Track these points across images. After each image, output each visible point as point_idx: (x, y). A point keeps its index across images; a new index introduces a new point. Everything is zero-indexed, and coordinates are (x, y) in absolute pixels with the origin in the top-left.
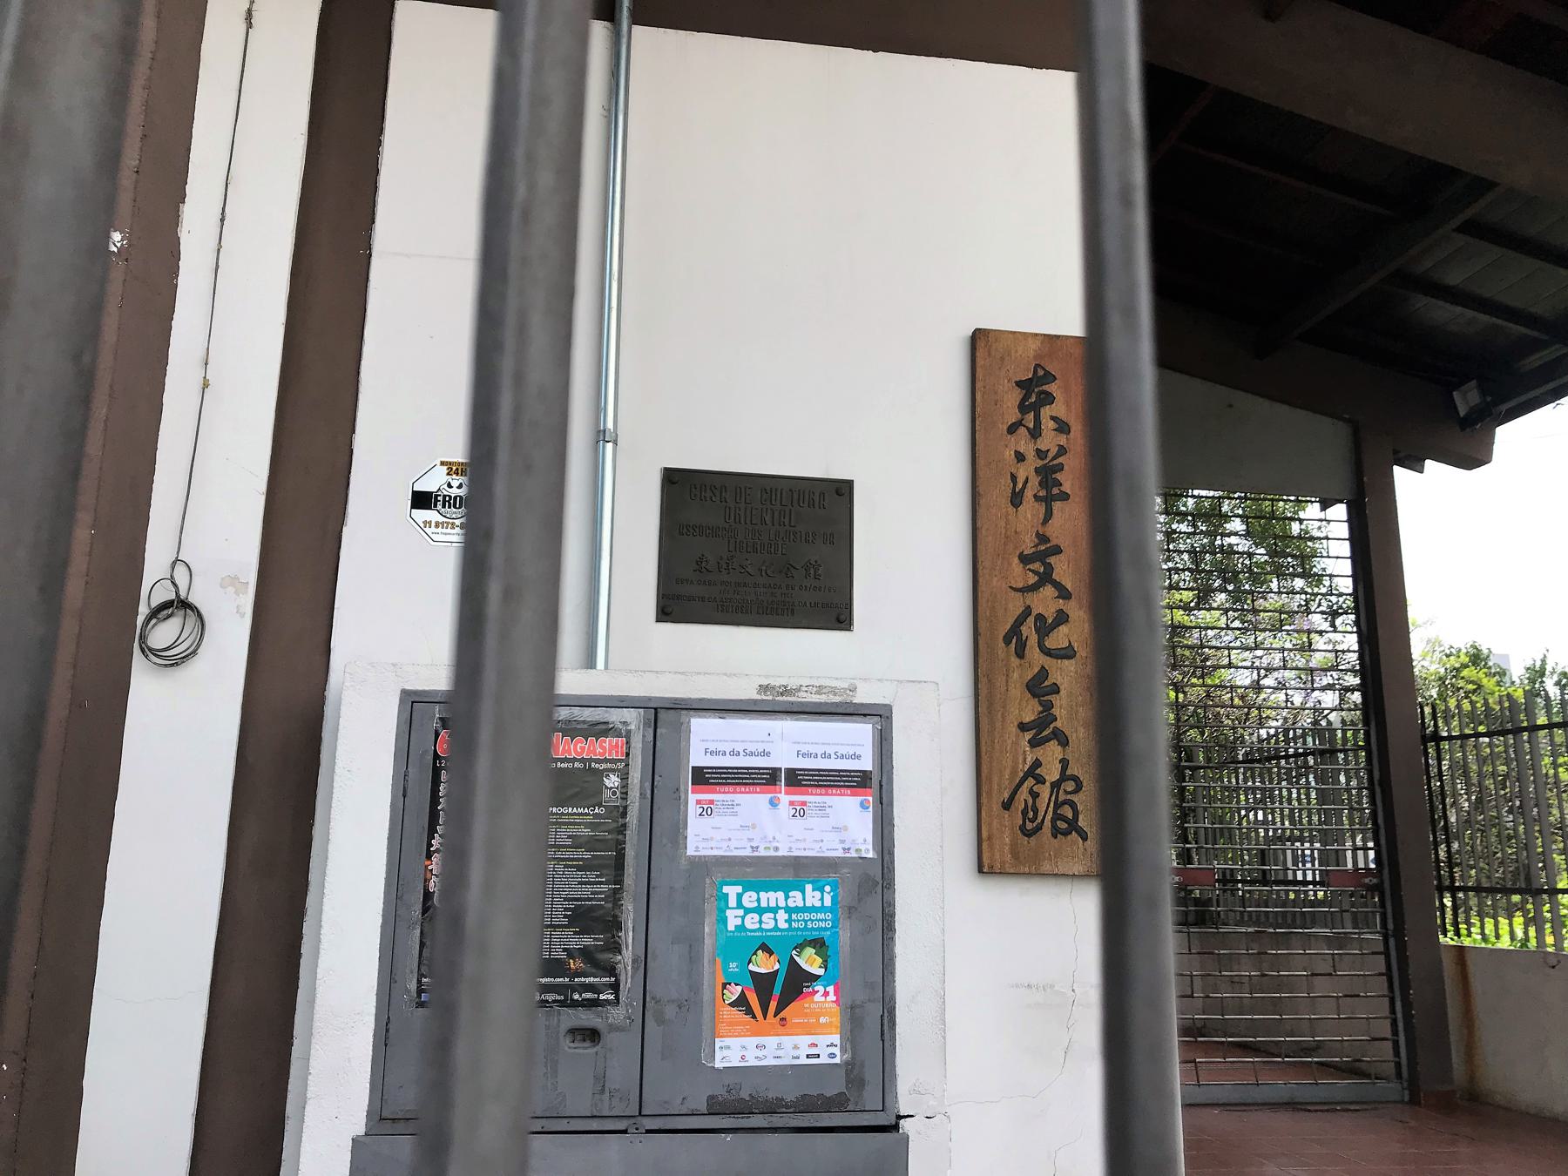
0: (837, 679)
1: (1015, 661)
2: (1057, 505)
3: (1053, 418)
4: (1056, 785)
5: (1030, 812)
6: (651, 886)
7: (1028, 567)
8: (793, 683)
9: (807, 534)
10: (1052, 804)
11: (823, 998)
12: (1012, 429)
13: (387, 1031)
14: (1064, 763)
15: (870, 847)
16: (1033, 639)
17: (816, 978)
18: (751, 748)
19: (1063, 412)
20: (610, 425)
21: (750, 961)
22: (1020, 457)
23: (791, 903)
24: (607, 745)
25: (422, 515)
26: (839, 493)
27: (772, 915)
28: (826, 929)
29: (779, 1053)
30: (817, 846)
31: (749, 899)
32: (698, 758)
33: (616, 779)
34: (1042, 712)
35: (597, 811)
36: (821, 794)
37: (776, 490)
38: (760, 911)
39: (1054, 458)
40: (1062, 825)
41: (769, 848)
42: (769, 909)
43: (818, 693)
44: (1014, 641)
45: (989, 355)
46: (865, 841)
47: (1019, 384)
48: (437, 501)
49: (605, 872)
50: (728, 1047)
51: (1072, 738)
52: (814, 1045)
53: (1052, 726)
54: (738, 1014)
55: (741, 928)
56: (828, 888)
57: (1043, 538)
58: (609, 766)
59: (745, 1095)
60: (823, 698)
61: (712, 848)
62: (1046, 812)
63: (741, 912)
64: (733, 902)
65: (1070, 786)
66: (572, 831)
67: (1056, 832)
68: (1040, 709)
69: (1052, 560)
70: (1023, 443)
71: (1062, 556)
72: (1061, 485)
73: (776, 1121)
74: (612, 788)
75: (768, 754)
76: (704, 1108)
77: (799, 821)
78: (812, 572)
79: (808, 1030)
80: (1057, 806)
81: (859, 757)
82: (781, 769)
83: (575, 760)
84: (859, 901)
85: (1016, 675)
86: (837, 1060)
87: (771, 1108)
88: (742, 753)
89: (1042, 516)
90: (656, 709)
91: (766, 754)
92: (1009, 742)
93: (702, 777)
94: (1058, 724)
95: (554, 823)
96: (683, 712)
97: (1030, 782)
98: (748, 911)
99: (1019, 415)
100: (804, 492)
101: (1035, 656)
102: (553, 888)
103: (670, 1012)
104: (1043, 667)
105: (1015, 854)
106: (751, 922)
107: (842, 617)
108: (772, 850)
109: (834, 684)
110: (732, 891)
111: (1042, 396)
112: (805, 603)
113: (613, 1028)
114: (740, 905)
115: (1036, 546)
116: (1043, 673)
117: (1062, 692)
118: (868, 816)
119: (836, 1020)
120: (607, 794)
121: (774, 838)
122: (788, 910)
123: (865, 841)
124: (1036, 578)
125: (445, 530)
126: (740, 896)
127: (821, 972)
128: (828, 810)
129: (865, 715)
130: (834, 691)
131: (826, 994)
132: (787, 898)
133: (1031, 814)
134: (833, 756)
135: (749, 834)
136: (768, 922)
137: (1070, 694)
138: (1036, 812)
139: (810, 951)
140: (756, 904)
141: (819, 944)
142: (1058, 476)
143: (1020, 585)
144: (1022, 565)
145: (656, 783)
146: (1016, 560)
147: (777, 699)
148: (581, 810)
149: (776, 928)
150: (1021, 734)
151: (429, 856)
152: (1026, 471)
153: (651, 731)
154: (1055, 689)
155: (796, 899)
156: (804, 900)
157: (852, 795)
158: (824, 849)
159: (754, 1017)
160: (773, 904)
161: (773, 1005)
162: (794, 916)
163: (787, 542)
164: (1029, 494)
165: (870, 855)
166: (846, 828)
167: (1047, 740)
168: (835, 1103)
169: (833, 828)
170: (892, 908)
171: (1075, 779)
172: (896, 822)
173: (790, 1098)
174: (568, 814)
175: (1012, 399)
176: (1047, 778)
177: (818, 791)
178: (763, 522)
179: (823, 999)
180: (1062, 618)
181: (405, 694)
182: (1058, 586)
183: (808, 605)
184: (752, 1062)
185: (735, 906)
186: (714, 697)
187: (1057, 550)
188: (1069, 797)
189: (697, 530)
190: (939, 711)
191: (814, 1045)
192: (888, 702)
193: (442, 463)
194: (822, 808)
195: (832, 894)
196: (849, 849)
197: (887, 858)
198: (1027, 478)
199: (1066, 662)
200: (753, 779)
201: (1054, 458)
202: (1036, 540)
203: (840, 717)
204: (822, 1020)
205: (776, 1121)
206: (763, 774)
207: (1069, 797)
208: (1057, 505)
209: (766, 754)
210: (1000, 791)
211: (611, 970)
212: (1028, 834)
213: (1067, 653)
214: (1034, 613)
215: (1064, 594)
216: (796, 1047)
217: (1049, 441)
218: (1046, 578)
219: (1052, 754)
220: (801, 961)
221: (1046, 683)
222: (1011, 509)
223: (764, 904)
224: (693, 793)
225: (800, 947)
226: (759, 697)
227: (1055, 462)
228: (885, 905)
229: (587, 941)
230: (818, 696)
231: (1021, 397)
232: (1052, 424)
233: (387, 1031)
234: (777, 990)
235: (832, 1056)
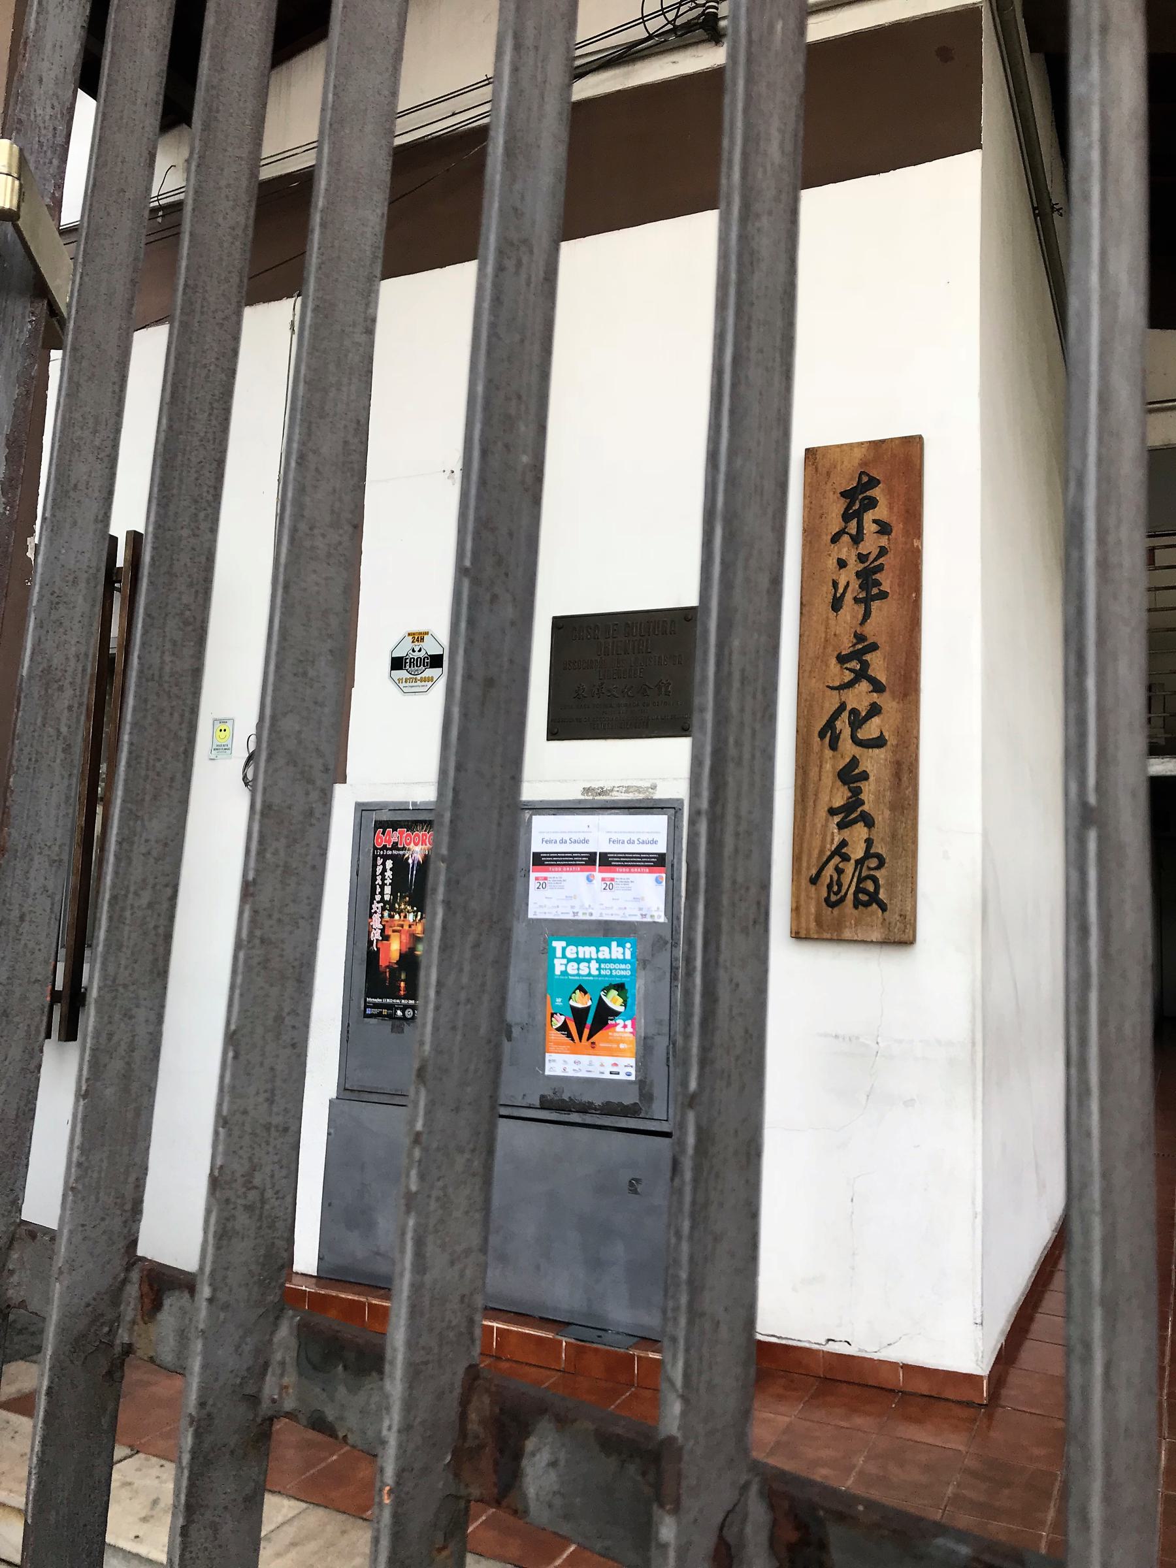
1: (828, 753)
2: (875, 605)
3: (875, 521)
4: (860, 863)
7: (845, 666)
8: (607, 786)
10: (855, 880)
11: (622, 1030)
12: (835, 539)
13: (348, 1032)
14: (869, 842)
15: (663, 914)
16: (847, 732)
17: (616, 1014)
18: (575, 837)
19: (885, 513)
21: (571, 998)
22: (842, 564)
23: (601, 956)
25: (398, 674)
27: (586, 964)
28: (626, 977)
29: (590, 1068)
31: (571, 952)
32: (537, 846)
34: (851, 798)
38: (578, 961)
39: (875, 560)
42: (584, 960)
43: (626, 792)
44: (829, 734)
45: (817, 471)
47: (844, 494)
48: (406, 663)
50: (554, 1061)
51: (878, 819)
52: (615, 1065)
53: (859, 810)
54: (561, 1037)
55: (565, 973)
56: (628, 945)
57: (860, 638)
59: (565, 1097)
60: (630, 796)
62: (849, 886)
63: (565, 961)
65: (873, 863)
67: (857, 903)
68: (850, 794)
69: (868, 657)
70: (845, 550)
71: (878, 653)
72: (880, 584)
73: (588, 1119)
75: (587, 842)
76: (537, 1104)
78: (663, 689)
79: (611, 1052)
80: (860, 881)
81: (656, 842)
82: (595, 853)
85: (828, 767)
86: (633, 1078)
87: (585, 1109)
89: (860, 617)
91: (586, 841)
92: (819, 825)
93: (540, 860)
94: (866, 808)
97: (837, 859)
98: (569, 960)
99: (843, 524)
101: (848, 748)
103: (516, 1032)
104: (854, 757)
105: (819, 922)
106: (572, 969)
109: (639, 784)
110: (558, 945)
111: (866, 502)
114: (564, 956)
115: (854, 645)
116: (854, 762)
117: (872, 778)
122: (598, 961)
124: (852, 675)
125: (411, 684)
126: (564, 949)
127: (621, 1009)
128: (631, 885)
129: (662, 808)
130: (638, 790)
131: (625, 1026)
132: (598, 951)
133: (835, 888)
136: (584, 970)
137: (878, 781)
138: (840, 885)
139: (613, 993)
140: (575, 956)
141: (620, 988)
142: (877, 576)
143: (837, 684)
144: (839, 666)
146: (834, 661)
149: (589, 974)
150: (831, 818)
151: (371, 917)
152: (846, 576)
154: (865, 776)
155: (604, 953)
159: (573, 1040)
160: (587, 956)
161: (586, 1032)
162: (603, 966)
164: (849, 597)
165: (662, 919)
166: (643, 899)
167: (854, 822)
171: (878, 856)
173: (598, 1102)
175: (836, 508)
176: (852, 856)
179: (622, 1030)
180: (875, 710)
181: (358, 805)
184: (570, 1073)
187: (874, 647)
188: (872, 873)
191: (615, 1065)
193: (409, 634)
194: (626, 882)
197: (675, 922)
198: (848, 583)
199: (876, 751)
201: (875, 560)
202: (855, 641)
204: (622, 1046)
205: (588, 1119)
207: (872, 873)
208: (875, 605)
209: (586, 841)
210: (808, 868)
213: (878, 742)
214: (849, 707)
215: (878, 687)
216: (602, 1065)
217: (871, 543)
218: (862, 674)
219: (860, 832)
220: (607, 1000)
221: (857, 771)
222: (832, 614)
223: (581, 956)
225: (607, 989)
226: (582, 797)
227: (876, 563)
231: (845, 506)
232: (874, 527)
233: (348, 1032)
234: (589, 1021)
235: (629, 1074)
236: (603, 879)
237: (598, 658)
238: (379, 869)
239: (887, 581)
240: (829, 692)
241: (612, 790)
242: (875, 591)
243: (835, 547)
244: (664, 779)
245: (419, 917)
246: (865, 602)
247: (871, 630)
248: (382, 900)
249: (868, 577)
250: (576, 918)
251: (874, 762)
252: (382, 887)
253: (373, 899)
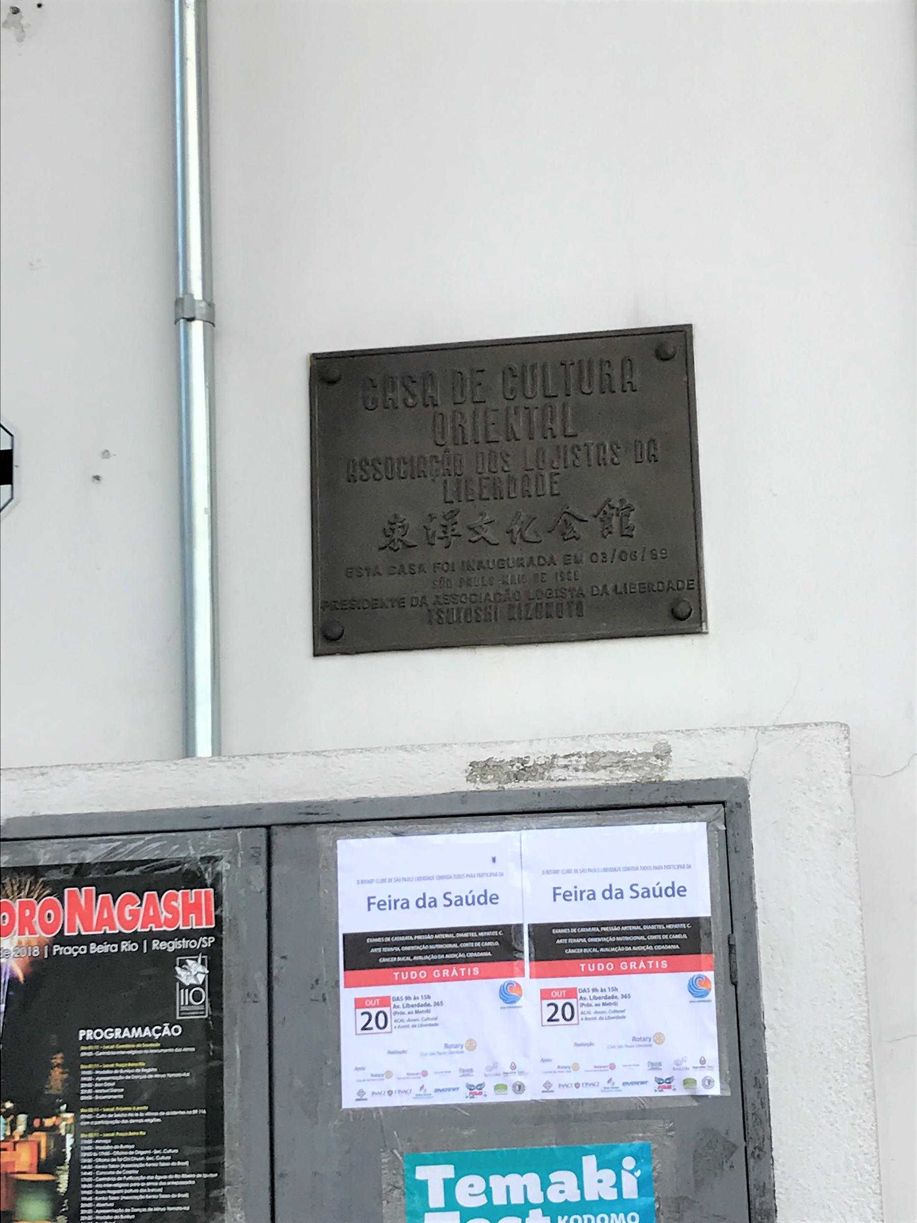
0: (628, 736)
6: (277, 1172)
8: (537, 753)
9: (601, 446)
15: (715, 1075)
18: (459, 888)
20: (197, 290)
23: (554, 1196)
24: (178, 904)
26: (663, 356)
30: (602, 1078)
33: (200, 968)
35: (166, 1031)
36: (606, 973)
37: (533, 367)
41: (505, 1087)
43: (590, 768)
46: (703, 1061)
49: (189, 1151)
56: (629, 1163)
58: (185, 944)
60: (601, 778)
61: (390, 1093)
64: (436, 1198)
66: (125, 1072)
74: (191, 987)
75: (493, 899)
77: (562, 1029)
78: (615, 521)
81: (681, 891)
82: (519, 927)
83: (117, 938)
84: (699, 1184)
88: (441, 901)
90: (268, 827)
95: (87, 1061)
96: (323, 828)
100: (590, 362)
102: (94, 1183)
107: (682, 609)
108: (510, 1088)
109: (624, 746)
112: (605, 587)
114: (451, 1204)
118: (708, 1010)
120: (183, 998)
121: (513, 1067)
123: (703, 1061)
126: (449, 1186)
128: (622, 1004)
129: (690, 805)
130: (622, 761)
132: (545, 1185)
134: (628, 893)
135: (465, 1060)
140: (482, 1201)
145: (275, 972)
147: (506, 787)
148: (137, 1033)
153: (261, 870)
156: (581, 1187)
157: (671, 969)
158: (618, 1084)
160: (517, 1199)
163: (561, 470)
165: (715, 1090)
166: (659, 1039)
169: (634, 1039)
170: (768, 1197)
172: (769, 1018)
174: (114, 1041)
177: (601, 966)
178: (511, 436)
183: (610, 588)
185: (443, 1206)
186: (383, 795)
189: (381, 468)
190: (850, 783)
192: (735, 773)
194: (609, 999)
195: (638, 1174)
196: (669, 1080)
197: (751, 1094)
200: (465, 950)
203: (640, 813)
206: (486, 939)
223: (499, 1199)
224: (346, 986)
226: (471, 787)
228: (753, 1192)
230: (591, 775)
236: (545, 994)
237: (439, 452)
241: (550, 765)
244: (688, 732)
245: (21, 1128)
250: (478, 1100)
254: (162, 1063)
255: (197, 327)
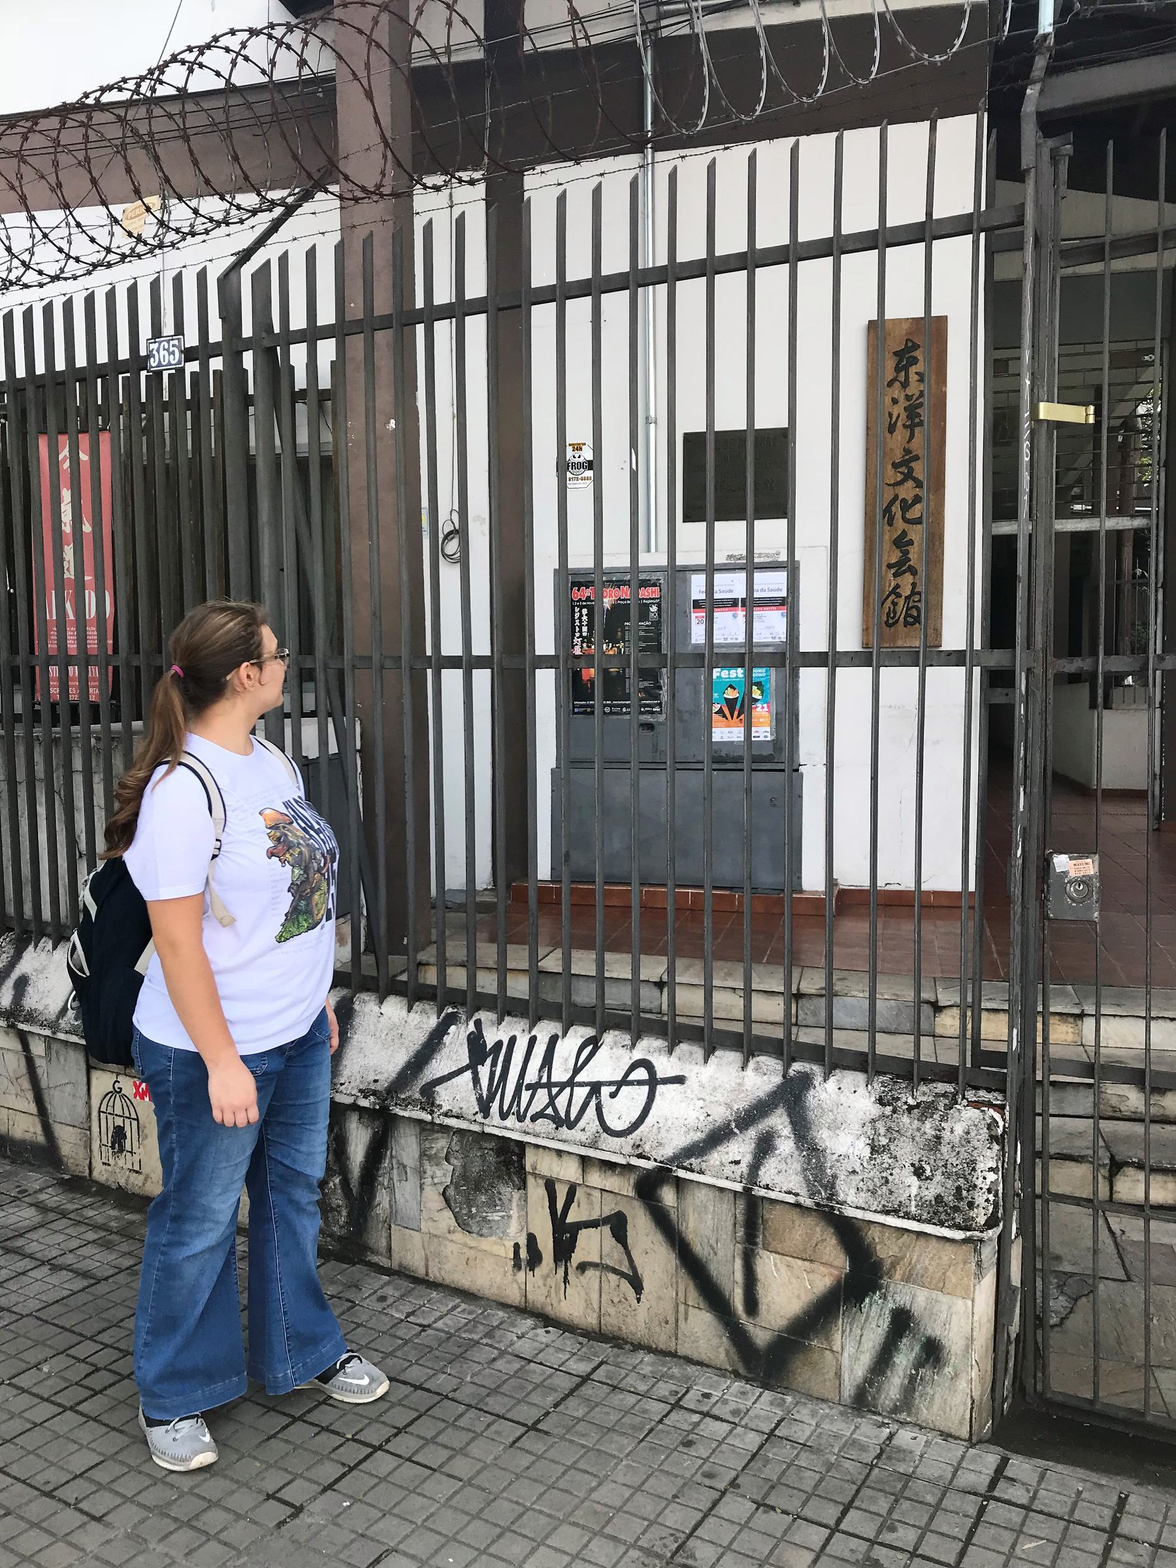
1: (887, 528)
2: (917, 430)
4: (908, 598)
5: (892, 614)
12: (890, 384)
14: (914, 585)
16: (899, 514)
22: (895, 401)
40: (910, 620)
47: (895, 353)
57: (907, 451)
59: (723, 754)
67: (906, 624)
69: (913, 464)
70: (896, 392)
71: (919, 462)
85: (887, 537)
86: (769, 739)
91: (731, 591)
94: (911, 563)
101: (900, 524)
103: (686, 716)
113: (660, 724)
116: (904, 533)
117: (916, 544)
119: (767, 720)
120: (652, 615)
130: (767, 555)
138: (895, 613)
154: (911, 543)
161: (736, 713)
164: (899, 424)
167: (904, 572)
168: (768, 759)
171: (919, 593)
175: (890, 364)
180: (917, 499)
182: (915, 480)
184: (726, 739)
187: (917, 458)
208: (917, 430)
209: (731, 591)
211: (657, 697)
212: (889, 626)
213: (918, 521)
215: (919, 485)
217: (914, 389)
218: (909, 476)
219: (908, 578)
229: (646, 684)
232: (916, 377)
238: (577, 615)
239: (924, 412)
240: (887, 488)
242: (917, 420)
243: (890, 390)
246: (911, 428)
247: (917, 445)
248: (581, 636)
249: (912, 411)
251: (916, 534)
252: (580, 627)
253: (573, 636)
254: (645, 631)
255: (652, 426)
